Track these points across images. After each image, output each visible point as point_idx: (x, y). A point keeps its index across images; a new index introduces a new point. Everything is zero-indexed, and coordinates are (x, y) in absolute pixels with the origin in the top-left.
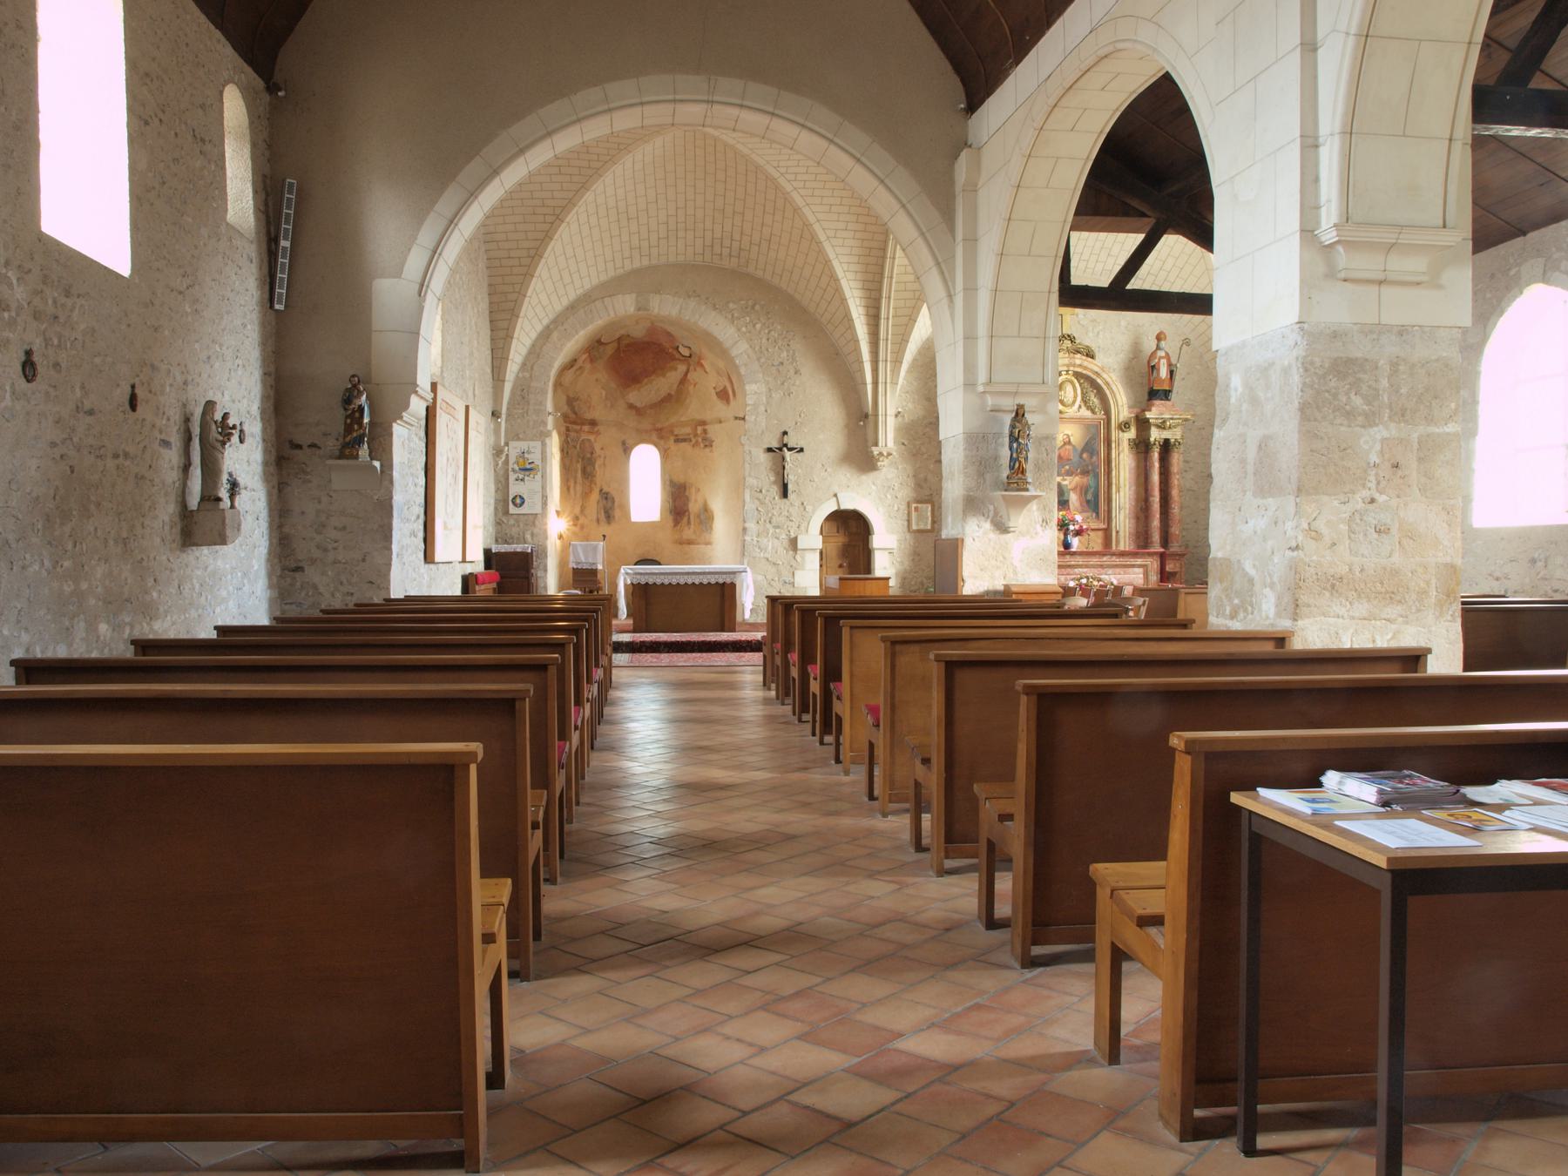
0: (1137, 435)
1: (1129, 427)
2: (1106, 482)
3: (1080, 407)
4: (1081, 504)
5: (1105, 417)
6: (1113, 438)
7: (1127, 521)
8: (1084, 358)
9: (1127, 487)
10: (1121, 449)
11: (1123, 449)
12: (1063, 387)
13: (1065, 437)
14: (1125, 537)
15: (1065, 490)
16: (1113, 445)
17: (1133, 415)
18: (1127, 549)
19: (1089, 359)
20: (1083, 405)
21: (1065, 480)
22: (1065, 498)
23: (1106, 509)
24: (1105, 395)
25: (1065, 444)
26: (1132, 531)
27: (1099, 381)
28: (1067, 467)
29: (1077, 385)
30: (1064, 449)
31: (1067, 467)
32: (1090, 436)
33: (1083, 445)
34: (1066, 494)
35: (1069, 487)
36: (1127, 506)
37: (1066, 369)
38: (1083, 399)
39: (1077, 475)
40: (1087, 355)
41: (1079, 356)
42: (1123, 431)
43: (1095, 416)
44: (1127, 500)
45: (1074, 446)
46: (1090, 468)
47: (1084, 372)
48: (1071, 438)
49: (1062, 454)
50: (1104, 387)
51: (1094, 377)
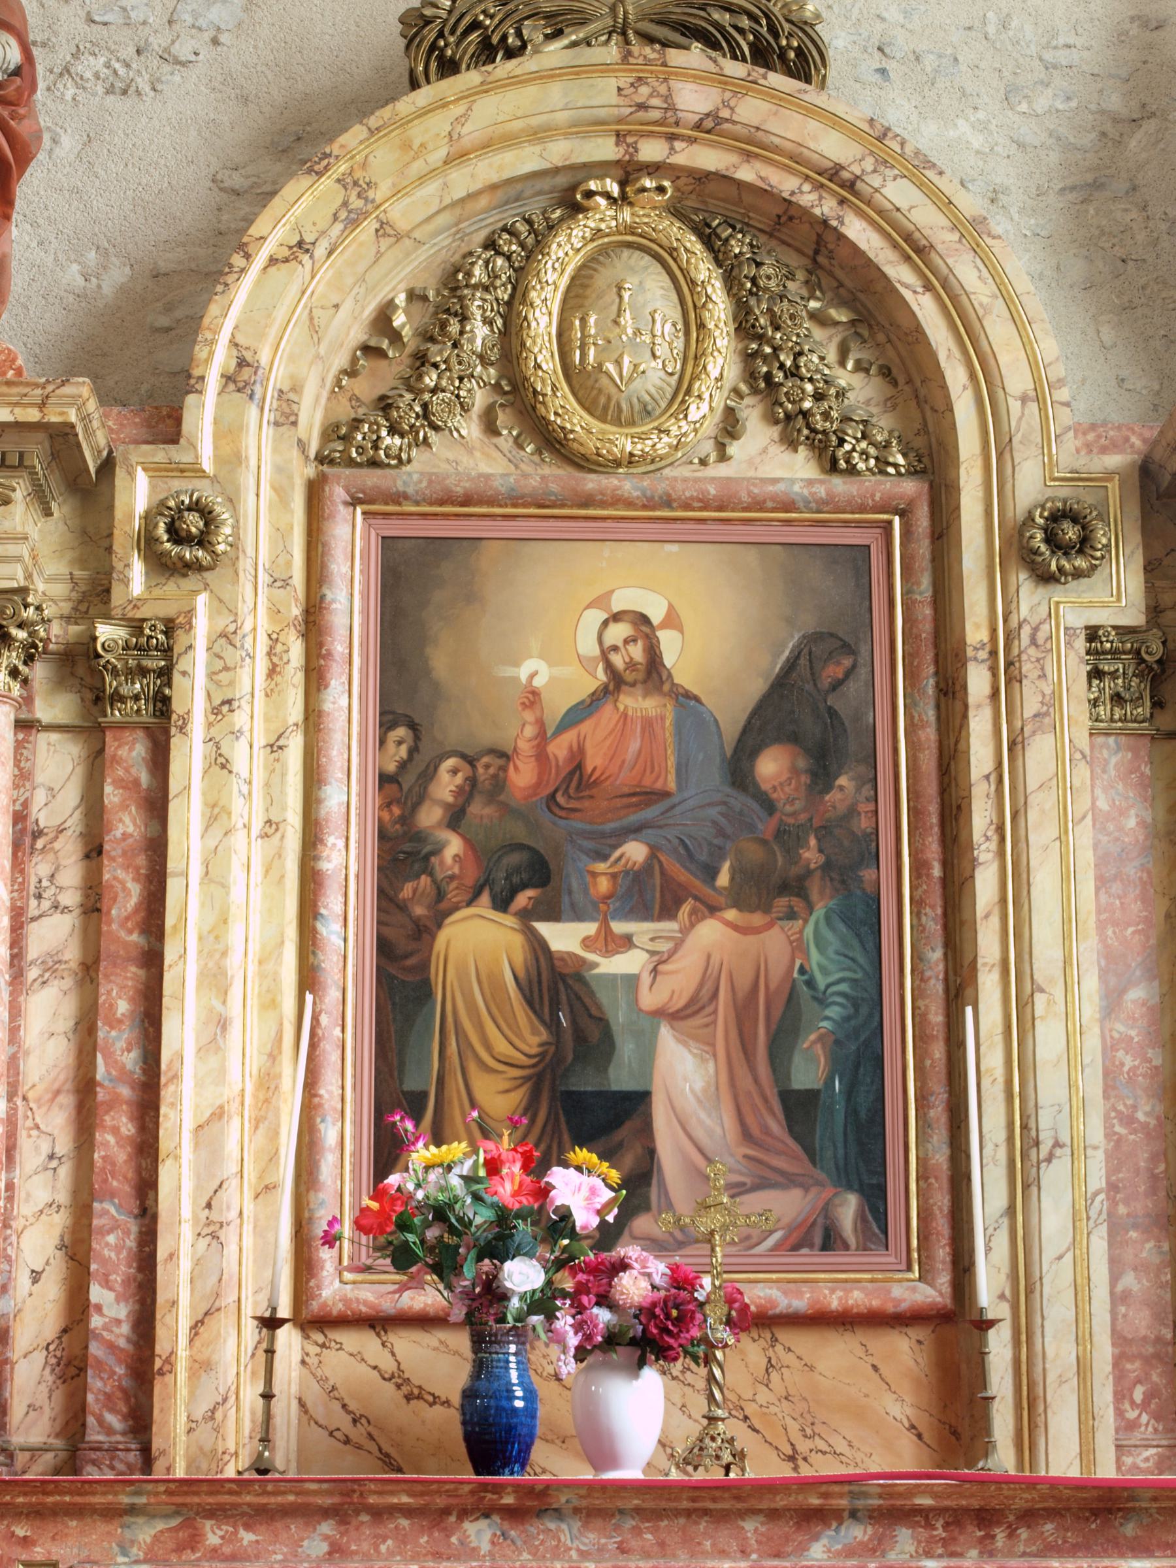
0: (1154, 611)
1: (1084, 544)
2: (936, 955)
3: (730, 427)
4: (746, 1135)
5: (910, 487)
6: (975, 632)
7: (1099, 1245)
8: (735, 69)
9: (1091, 984)
10: (1031, 705)
11: (1052, 702)
12: (603, 278)
13: (618, 632)
14: (1083, 1368)
15: (619, 1017)
16: (977, 681)
17: (1114, 461)
18: (1106, 1470)
19: (777, 80)
20: (751, 413)
21: (627, 942)
22: (620, 1079)
23: (940, 1157)
24: (917, 334)
25: (616, 682)
26: (1141, 1322)
27: (857, 230)
28: (635, 851)
29: (704, 269)
30: (607, 715)
31: (635, 851)
32: (809, 622)
33: (756, 687)
34: (626, 1049)
35: (649, 999)
36: (1095, 1132)
37: (606, 149)
38: (750, 376)
39: (713, 910)
40: (762, 56)
41: (695, 56)
42: (1045, 578)
43: (839, 485)
44: (1092, 1084)
45: (685, 698)
46: (811, 854)
47: (746, 174)
48: (670, 645)
49: (594, 761)
50: (901, 274)
51: (826, 207)
